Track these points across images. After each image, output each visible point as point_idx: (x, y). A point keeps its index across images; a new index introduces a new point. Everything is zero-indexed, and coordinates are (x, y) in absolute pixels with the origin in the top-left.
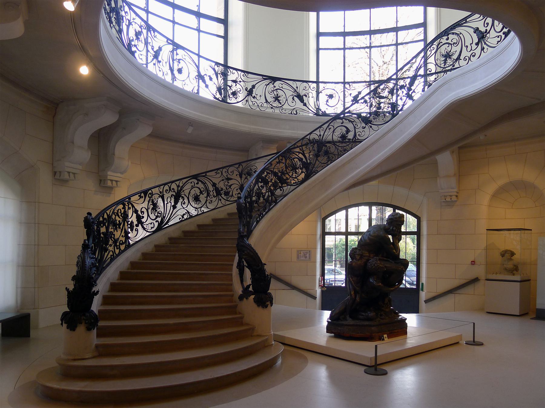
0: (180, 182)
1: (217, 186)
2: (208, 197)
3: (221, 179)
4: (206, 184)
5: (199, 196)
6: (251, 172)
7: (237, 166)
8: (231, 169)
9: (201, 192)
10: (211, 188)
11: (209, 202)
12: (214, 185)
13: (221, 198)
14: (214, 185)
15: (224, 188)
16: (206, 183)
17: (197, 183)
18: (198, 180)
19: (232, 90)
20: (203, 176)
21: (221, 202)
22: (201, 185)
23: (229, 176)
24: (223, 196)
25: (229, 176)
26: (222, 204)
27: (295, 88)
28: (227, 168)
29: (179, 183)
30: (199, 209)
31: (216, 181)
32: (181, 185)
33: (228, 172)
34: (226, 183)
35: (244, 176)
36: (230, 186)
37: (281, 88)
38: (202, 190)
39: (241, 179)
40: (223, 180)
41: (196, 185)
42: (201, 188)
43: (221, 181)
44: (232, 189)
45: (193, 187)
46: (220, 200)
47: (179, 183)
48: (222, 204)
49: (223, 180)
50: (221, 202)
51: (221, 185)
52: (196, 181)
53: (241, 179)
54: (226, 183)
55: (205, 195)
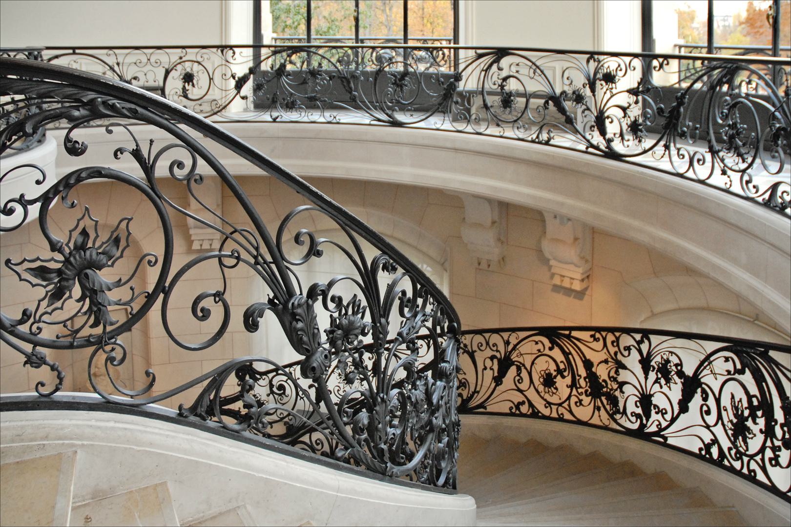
0: (510, 335)
1: (594, 370)
2: (574, 389)
3: (603, 356)
4: (570, 356)
5: (555, 377)
7: (638, 337)
8: (626, 340)
9: (560, 372)
10: (582, 372)
11: (576, 403)
12: (588, 364)
13: (600, 404)
14: (588, 364)
16: (570, 353)
17: (551, 349)
18: (553, 342)
19: (629, 119)
20: (565, 336)
21: (600, 416)
22: (557, 354)
23: (619, 357)
25: (619, 355)
26: (601, 421)
28: (617, 334)
29: (509, 337)
30: (554, 407)
31: (595, 357)
32: (513, 341)
33: (618, 346)
35: (652, 376)
36: (621, 385)
38: (562, 366)
39: (646, 378)
40: (606, 362)
41: (547, 352)
42: (558, 361)
45: (540, 354)
46: (599, 409)
47: (509, 337)
48: (601, 421)
50: (600, 416)
51: (602, 372)
52: (546, 341)
53: (646, 378)
54: (612, 374)
55: (568, 380)
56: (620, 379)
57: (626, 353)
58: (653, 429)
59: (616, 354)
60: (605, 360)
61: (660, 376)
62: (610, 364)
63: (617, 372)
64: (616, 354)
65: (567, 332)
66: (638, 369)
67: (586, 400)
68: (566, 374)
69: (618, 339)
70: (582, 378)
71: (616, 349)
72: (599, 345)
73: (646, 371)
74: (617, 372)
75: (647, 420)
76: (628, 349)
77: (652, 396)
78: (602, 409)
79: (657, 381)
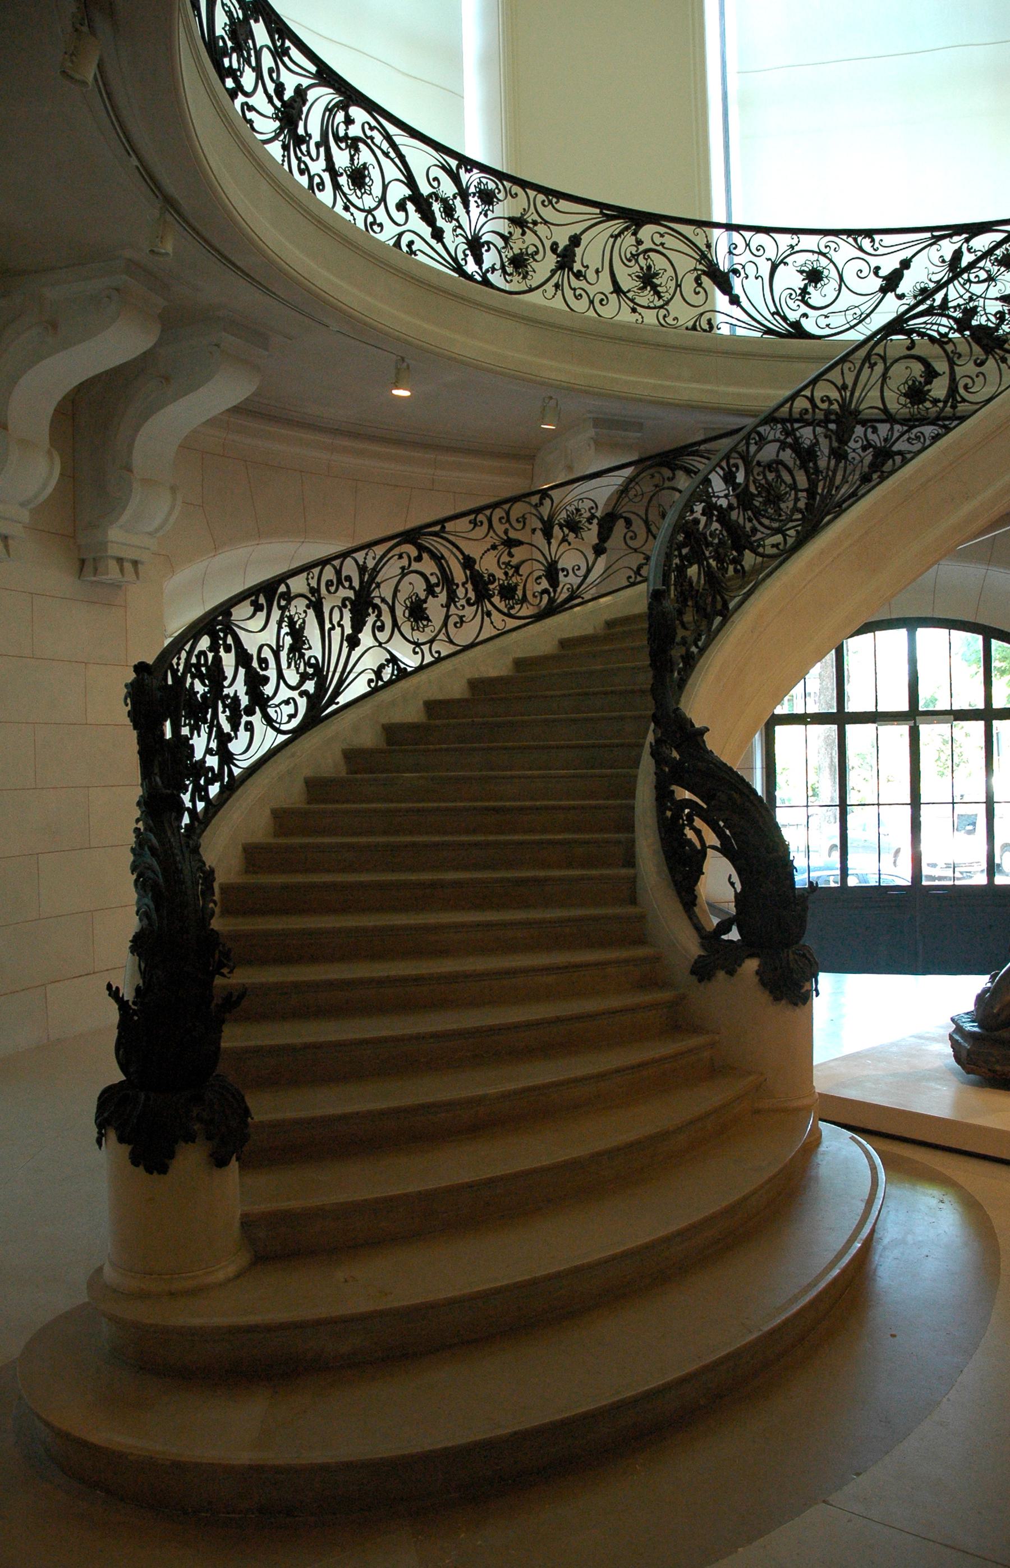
1: (477, 567)
4: (443, 561)
6: (577, 518)
8: (518, 509)
12: (468, 563)
14: (468, 563)
15: (499, 574)
16: (443, 557)
21: (492, 623)
23: (513, 534)
24: (496, 600)
27: (704, 248)
33: (508, 521)
34: (505, 558)
36: (517, 568)
37: (660, 248)
39: (549, 543)
43: (488, 550)
44: (524, 578)
46: (489, 614)
49: (494, 547)
50: (492, 623)
51: (488, 565)
53: (549, 543)
54: (505, 558)
56: (514, 561)
57: (519, 526)
58: (565, 595)
59: (506, 532)
60: (492, 546)
61: (566, 531)
62: (500, 548)
63: (511, 555)
64: (506, 532)
65: (437, 528)
66: (539, 539)
67: (469, 611)
68: (438, 590)
69: (508, 513)
70: (460, 586)
71: (507, 526)
72: (481, 531)
73: (548, 535)
74: (511, 555)
75: (555, 592)
76: (523, 520)
77: (556, 562)
78: (494, 612)
79: (564, 540)
